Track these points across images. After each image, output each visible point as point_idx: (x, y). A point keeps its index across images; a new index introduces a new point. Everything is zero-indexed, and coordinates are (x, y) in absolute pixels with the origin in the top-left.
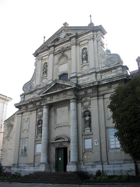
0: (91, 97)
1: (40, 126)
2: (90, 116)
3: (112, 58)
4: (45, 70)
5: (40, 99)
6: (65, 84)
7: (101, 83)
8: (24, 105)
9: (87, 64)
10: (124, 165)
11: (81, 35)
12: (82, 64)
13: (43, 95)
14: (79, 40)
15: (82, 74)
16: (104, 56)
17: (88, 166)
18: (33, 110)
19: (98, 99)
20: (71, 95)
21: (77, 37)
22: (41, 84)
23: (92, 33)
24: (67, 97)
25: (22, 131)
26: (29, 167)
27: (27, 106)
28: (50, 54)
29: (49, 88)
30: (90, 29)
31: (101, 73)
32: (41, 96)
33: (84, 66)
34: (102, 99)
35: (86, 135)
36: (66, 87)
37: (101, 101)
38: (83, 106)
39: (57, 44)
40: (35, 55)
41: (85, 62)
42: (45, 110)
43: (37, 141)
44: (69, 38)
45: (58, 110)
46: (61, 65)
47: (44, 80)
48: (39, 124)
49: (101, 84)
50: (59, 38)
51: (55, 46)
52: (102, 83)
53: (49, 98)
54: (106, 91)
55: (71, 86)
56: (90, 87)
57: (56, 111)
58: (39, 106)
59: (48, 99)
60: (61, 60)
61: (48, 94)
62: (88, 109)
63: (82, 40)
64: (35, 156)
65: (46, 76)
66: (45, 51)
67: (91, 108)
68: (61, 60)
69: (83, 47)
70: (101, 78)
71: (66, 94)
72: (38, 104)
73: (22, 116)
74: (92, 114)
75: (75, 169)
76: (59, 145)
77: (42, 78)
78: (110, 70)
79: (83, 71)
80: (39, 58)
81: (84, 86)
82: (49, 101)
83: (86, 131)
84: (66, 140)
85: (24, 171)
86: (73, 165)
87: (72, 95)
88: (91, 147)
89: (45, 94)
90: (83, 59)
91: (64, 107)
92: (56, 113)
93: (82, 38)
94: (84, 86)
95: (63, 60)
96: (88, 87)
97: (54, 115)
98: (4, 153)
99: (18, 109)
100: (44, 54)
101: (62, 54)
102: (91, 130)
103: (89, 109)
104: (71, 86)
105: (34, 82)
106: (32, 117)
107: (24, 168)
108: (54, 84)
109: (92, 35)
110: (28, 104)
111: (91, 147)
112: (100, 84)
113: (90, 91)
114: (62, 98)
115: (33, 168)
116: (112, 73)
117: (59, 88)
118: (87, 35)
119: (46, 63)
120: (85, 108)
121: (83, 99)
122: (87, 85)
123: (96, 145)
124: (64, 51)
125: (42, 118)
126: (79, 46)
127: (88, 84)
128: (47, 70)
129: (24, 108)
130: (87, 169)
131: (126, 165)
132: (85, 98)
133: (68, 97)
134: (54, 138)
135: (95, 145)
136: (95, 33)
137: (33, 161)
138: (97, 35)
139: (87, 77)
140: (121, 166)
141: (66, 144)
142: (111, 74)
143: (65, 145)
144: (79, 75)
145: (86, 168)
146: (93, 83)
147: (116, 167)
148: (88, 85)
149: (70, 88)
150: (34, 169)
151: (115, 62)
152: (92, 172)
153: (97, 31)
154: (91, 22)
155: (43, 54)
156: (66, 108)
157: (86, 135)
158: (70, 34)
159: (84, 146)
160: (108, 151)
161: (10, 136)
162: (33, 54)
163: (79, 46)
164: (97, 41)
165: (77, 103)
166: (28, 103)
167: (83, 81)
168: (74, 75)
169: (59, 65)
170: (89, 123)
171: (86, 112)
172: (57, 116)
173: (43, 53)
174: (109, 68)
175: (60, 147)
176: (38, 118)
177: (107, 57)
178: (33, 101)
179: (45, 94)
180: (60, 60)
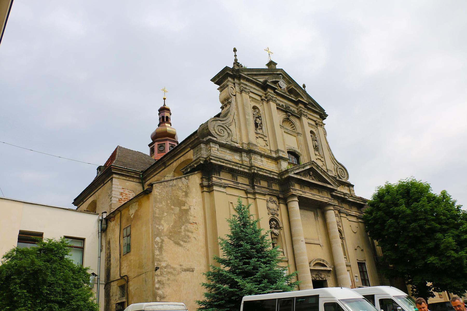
0: (340, 212)
5: (276, 177)
9: (323, 159)
11: (309, 109)
13: (296, 176)
23: (318, 117)
24: (325, 199)
32: (293, 176)
40: (231, 73)
41: (317, 153)
47: (260, 139)
54: (349, 211)
58: (268, 190)
59: (297, 187)
72: (264, 184)
76: (317, 275)
84: (329, 269)
89: (299, 177)
91: (307, 210)
93: (311, 115)
95: (287, 126)
98: (168, 279)
100: (254, 89)
128: (261, 123)
149: (332, 187)
155: (251, 87)
161: (183, 234)
169: (285, 132)
175: (318, 279)
178: (261, 173)
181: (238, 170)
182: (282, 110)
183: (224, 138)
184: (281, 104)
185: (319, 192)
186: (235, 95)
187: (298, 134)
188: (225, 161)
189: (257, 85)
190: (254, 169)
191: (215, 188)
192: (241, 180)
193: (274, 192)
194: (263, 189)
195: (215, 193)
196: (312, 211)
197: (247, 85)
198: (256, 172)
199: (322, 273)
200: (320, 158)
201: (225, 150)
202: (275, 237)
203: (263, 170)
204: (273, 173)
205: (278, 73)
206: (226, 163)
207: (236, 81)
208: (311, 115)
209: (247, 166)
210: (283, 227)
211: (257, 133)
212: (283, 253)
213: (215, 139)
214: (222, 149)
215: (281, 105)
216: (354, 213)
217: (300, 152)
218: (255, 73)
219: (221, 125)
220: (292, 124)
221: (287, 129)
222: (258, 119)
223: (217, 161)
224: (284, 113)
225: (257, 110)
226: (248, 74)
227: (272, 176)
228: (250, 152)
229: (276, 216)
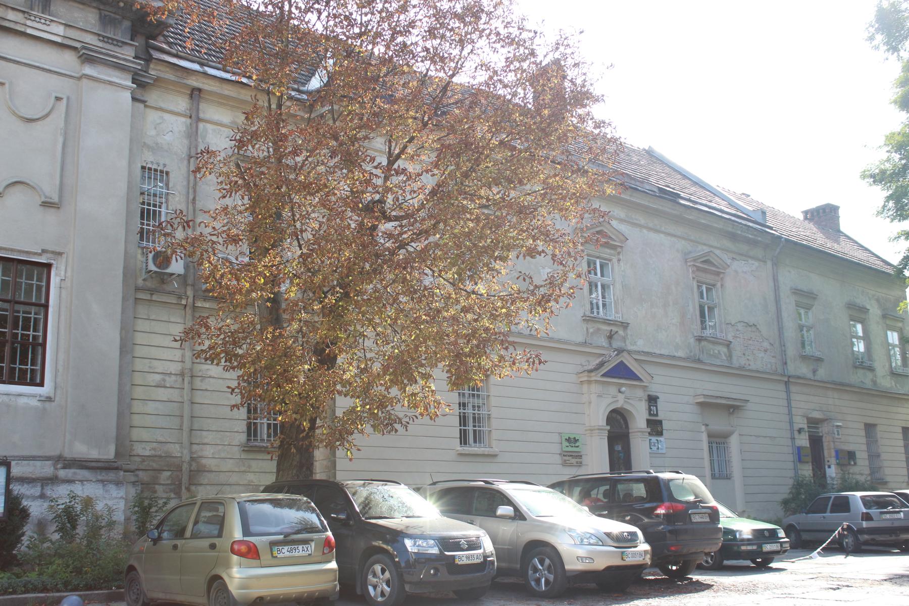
54: (11, 15)
140: (42, 496)
216: (60, 30)
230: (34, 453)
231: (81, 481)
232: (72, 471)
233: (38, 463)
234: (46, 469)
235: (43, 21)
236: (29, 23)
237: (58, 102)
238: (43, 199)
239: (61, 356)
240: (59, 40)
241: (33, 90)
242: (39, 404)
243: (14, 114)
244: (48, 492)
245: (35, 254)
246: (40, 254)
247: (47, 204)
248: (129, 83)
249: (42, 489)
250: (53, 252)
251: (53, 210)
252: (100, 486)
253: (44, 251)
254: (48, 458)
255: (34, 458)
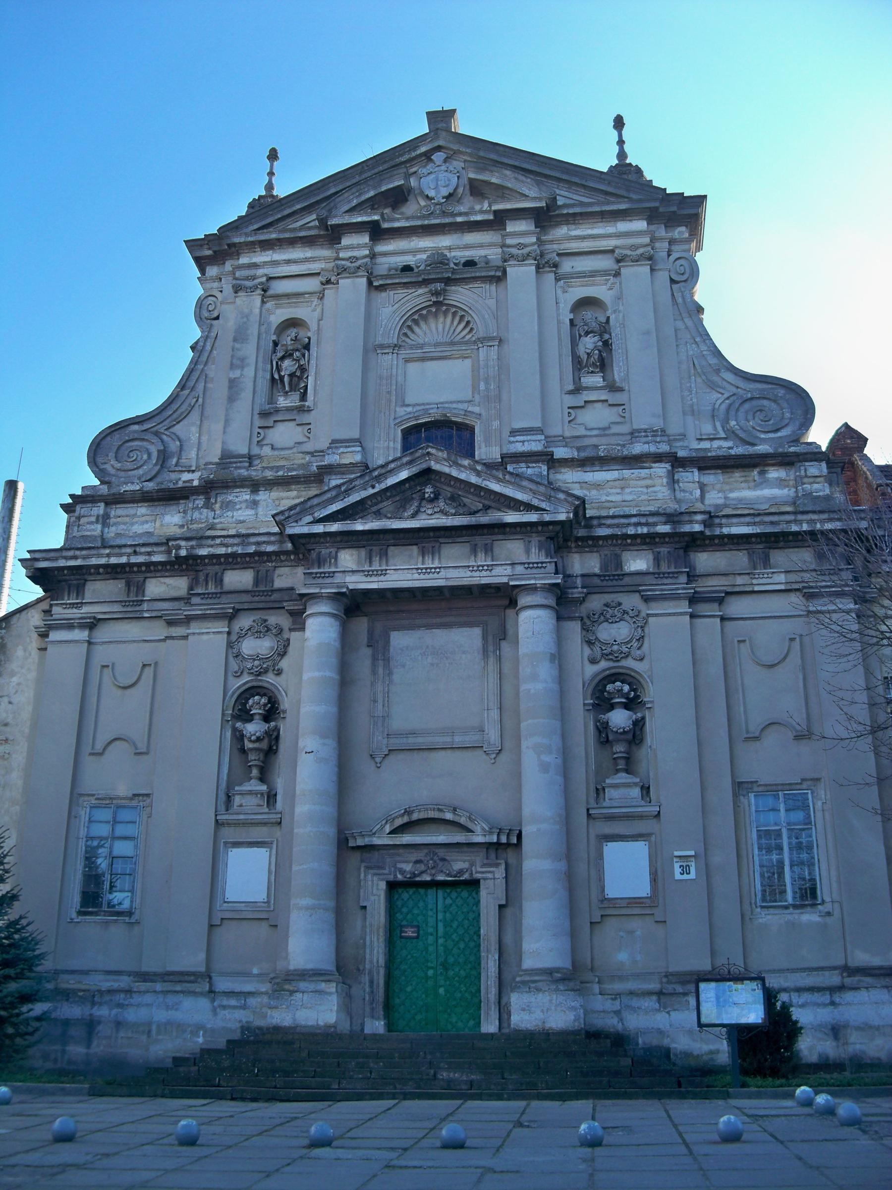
0: (647, 600)
1: (254, 728)
2: (632, 703)
3: (765, 403)
4: (288, 366)
5: (270, 548)
6: (495, 487)
7: (721, 526)
8: (113, 571)
10: (849, 996)
11: (573, 219)
12: (571, 387)
13: (319, 529)
14: (558, 241)
15: (579, 449)
16: (715, 378)
17: (635, 1002)
18: (203, 617)
19: (692, 616)
20: (529, 565)
21: (544, 217)
22: (256, 450)
23: (641, 225)
24: (498, 571)
25: (87, 749)
26: (171, 999)
27: (139, 578)
28: (342, 271)
29: (364, 494)
30: (634, 197)
31: (700, 469)
32: (305, 530)
33: (589, 406)
34: (718, 620)
35: (611, 818)
36: (487, 508)
37: (709, 627)
38: (590, 643)
39: (397, 225)
41: (596, 380)
42: (320, 629)
43: (228, 824)
44: (496, 213)
45: (400, 640)
46: (423, 359)
47: (281, 427)
48: (244, 715)
49: (717, 532)
50: (410, 190)
51: (377, 232)
52: (726, 531)
53: (354, 552)
54: (739, 580)
55: (529, 507)
56: (649, 541)
57: (387, 642)
58: (246, 598)
59: (347, 559)
60: (422, 323)
61: (359, 526)
62: (624, 663)
63: (574, 246)
64: (211, 926)
65: (301, 410)
66: (292, 242)
67: (645, 661)
68: (422, 323)
69: (580, 292)
70: (703, 497)
71: (488, 550)
72: (239, 579)
73: (90, 643)
74: (651, 693)
75: (571, 1016)
77: (264, 415)
78: (755, 466)
79: (582, 431)
80: (247, 278)
81: (609, 522)
82: (351, 570)
83: (610, 793)
84: (480, 839)
85: (118, 1024)
86: (557, 990)
87: (540, 565)
88: (644, 890)
89: (335, 527)
90: (578, 365)
92: (387, 661)
93: (583, 238)
94: (609, 522)
96: (634, 537)
97: (374, 672)
99: (37, 592)
100: (288, 262)
101: (437, 293)
102: (646, 790)
103: (630, 663)
104: (529, 507)
105: (188, 430)
106: (202, 661)
107: (120, 1005)
108: (404, 475)
109: (647, 240)
110: (152, 569)
111: (644, 890)
112: (708, 533)
113: (637, 563)
114: (455, 568)
115: (204, 1003)
116: (764, 483)
117: (441, 504)
118: (610, 229)
119: (293, 323)
120: (604, 656)
121: (595, 603)
122: (634, 520)
123: (685, 877)
124: (448, 281)
125: (270, 678)
126: (552, 276)
127: (643, 520)
128: (303, 369)
129: (101, 595)
130: (627, 1015)
131: (862, 996)
132: (608, 598)
133: (508, 570)
134: (389, 820)
135: (678, 876)
136: (661, 232)
137: (202, 956)
138: (672, 242)
139: (614, 474)
140: (833, 1003)
141: (472, 864)
142: (757, 486)
143: (466, 865)
144: (560, 452)
145: (618, 1013)
146: (672, 518)
147: (802, 1006)
148: (637, 525)
149: (533, 517)
150: (214, 1011)
151: (786, 425)
152: (660, 1032)
153: (671, 221)
154: (622, 155)
156: (466, 639)
157: (611, 818)
158: (502, 191)
159: (601, 879)
160: (747, 918)
162: (192, 245)
163: (557, 280)
164: (673, 281)
165: (559, 618)
166: (156, 558)
167: (617, 494)
168: (534, 445)
169: (407, 361)
170: (623, 749)
171: (613, 677)
172: (396, 677)
173: (278, 256)
174: (751, 450)
176: (238, 675)
177: (734, 390)
178: (203, 552)
179: (335, 527)
180: (409, 327)
181: (131, 565)
182: (405, 285)
183: (141, 472)
184: (409, 260)
185: (474, 551)
186: (217, 318)
187: (482, 340)
188: (78, 553)
189: (309, 242)
190: (179, 548)
191: (54, 636)
192: (155, 587)
193: (275, 596)
194: (224, 599)
195: (50, 648)
196: (471, 625)
197: (255, 266)
198: (183, 553)
199: (450, 855)
200: (603, 398)
201: (131, 511)
202: (251, 745)
203: (210, 542)
204: (253, 540)
205: (423, 149)
206: (84, 558)
207: (228, 266)
208: (583, 238)
209: (156, 544)
210: (284, 712)
211: (264, 415)
212: (271, 798)
213: (104, 490)
214: (120, 512)
215: (412, 263)
216: (782, 578)
217: (476, 409)
218: (298, 207)
219: (136, 436)
220: (462, 316)
221: (422, 346)
222: (287, 363)
223: (56, 559)
224: (420, 291)
225: (292, 332)
226: (259, 229)
227: (252, 549)
228: (209, 489)
229: (270, 678)
230: (822, 964)
231: (867, 988)
232: (856, 978)
233: (827, 973)
234: (834, 979)
235: (766, 576)
236: (755, 582)
237: (793, 644)
238: (795, 734)
239: (834, 873)
240: (782, 587)
241: (769, 637)
242: (818, 919)
243: (758, 664)
244: (837, 999)
245: (797, 784)
246: (801, 784)
247: (798, 737)
248: (852, 606)
249: (831, 996)
250: (811, 780)
251: (805, 741)
252: (885, 991)
253: (803, 780)
254: (834, 968)
255: (822, 969)
